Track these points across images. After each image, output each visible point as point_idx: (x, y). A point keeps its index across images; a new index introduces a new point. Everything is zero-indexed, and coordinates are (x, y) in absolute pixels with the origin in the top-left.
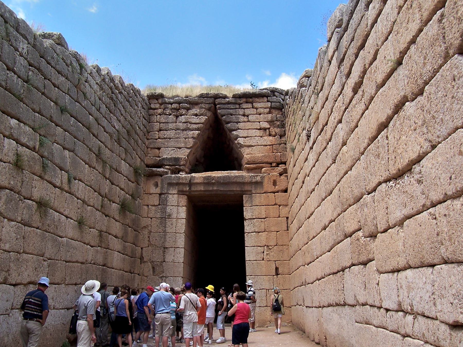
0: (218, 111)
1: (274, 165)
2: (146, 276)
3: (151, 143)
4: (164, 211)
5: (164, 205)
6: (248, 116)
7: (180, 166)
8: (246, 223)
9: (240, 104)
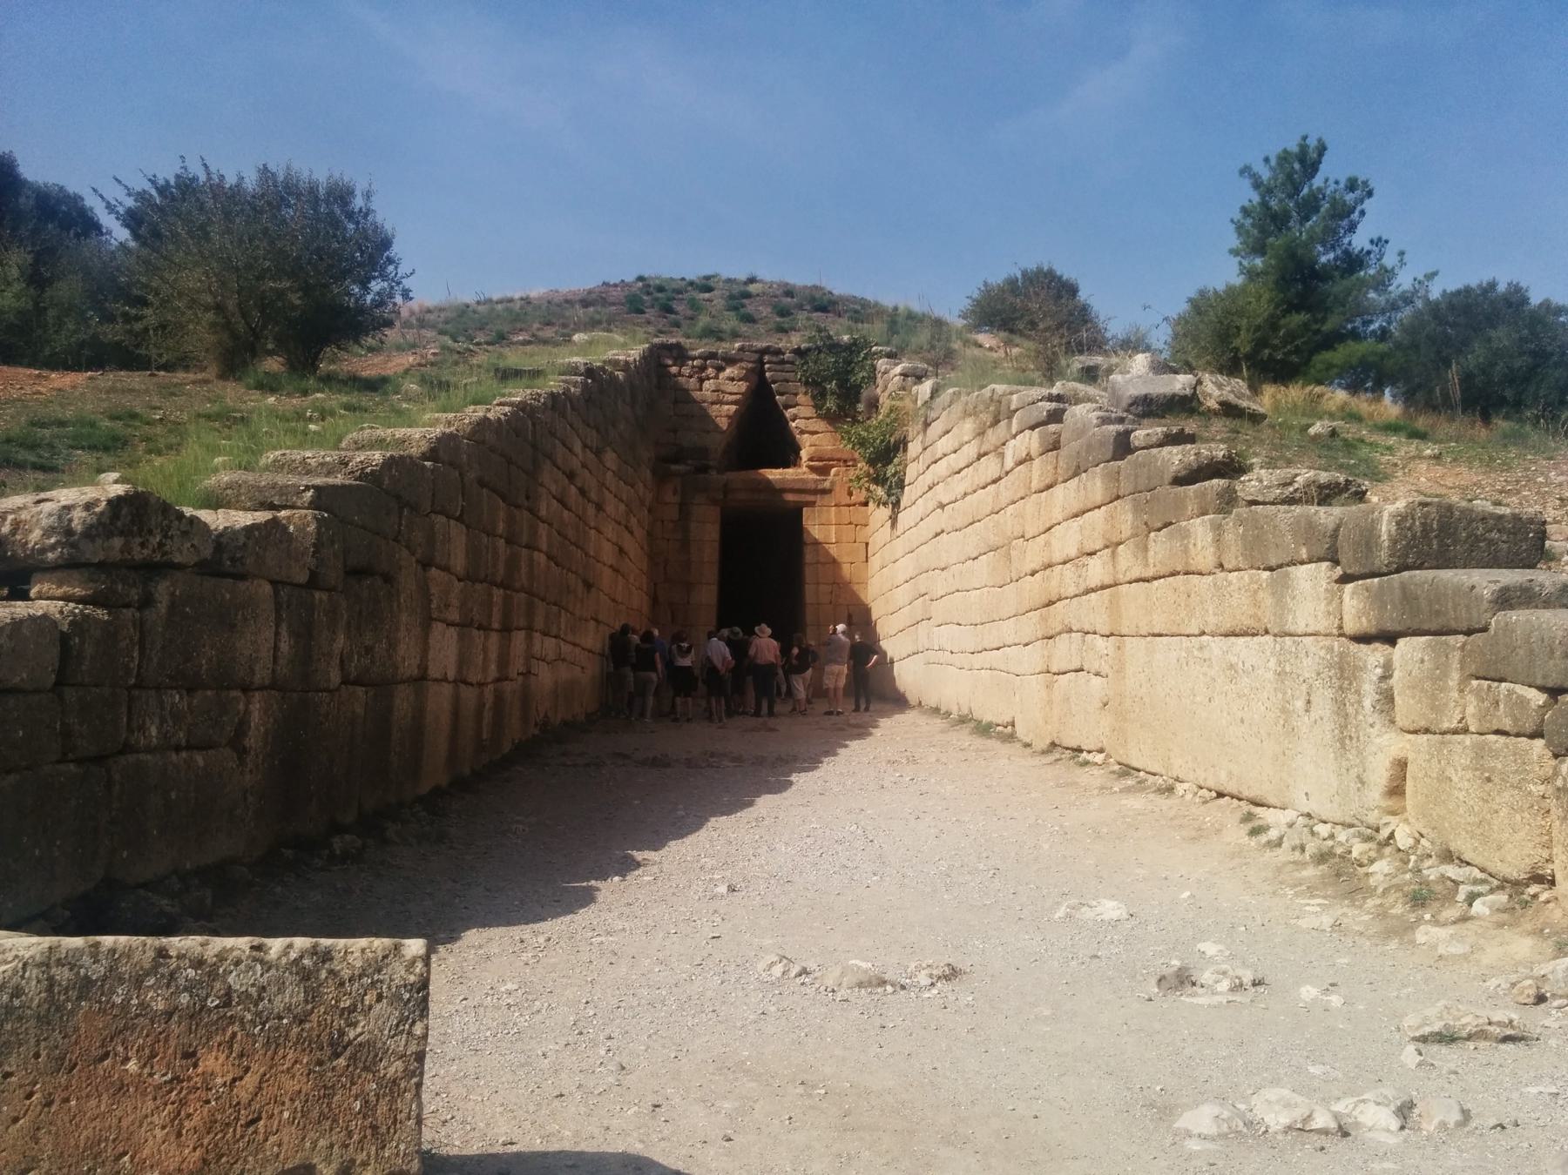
0: (768, 374)
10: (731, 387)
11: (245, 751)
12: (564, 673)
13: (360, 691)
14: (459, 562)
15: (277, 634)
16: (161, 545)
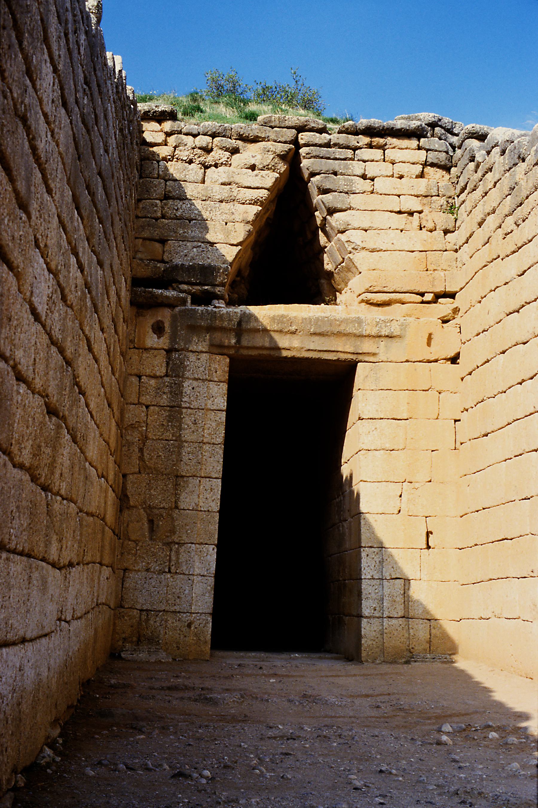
1: (429, 297)
2: (133, 541)
3: (143, 227)
4: (177, 392)
5: (177, 376)
6: (373, 180)
7: (214, 285)
9: (355, 149)
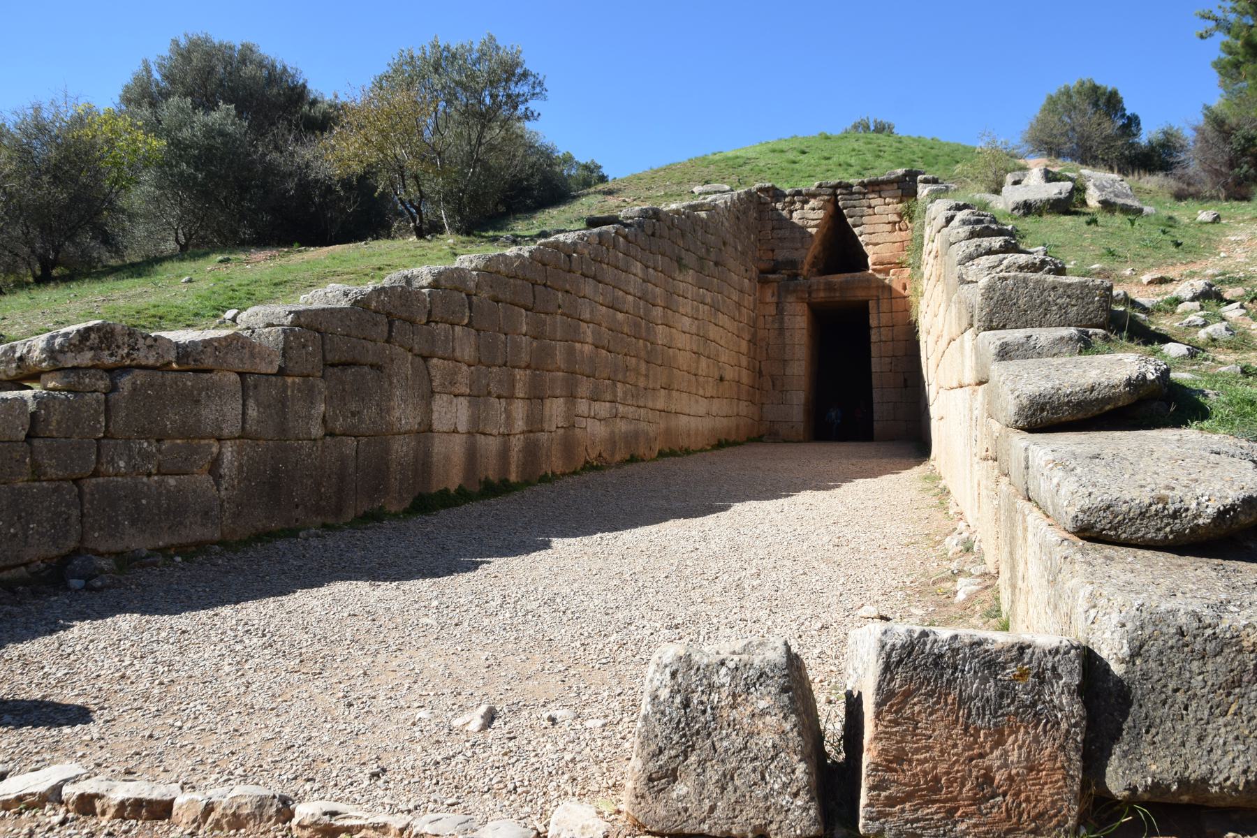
4: (782, 322)
8: (873, 332)
10: (812, 215)
11: (221, 476)
12: (622, 427)
13: (351, 442)
14: (466, 351)
15: (244, 405)
16: (128, 354)
